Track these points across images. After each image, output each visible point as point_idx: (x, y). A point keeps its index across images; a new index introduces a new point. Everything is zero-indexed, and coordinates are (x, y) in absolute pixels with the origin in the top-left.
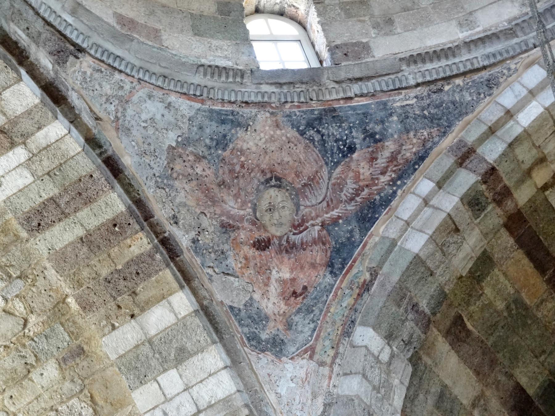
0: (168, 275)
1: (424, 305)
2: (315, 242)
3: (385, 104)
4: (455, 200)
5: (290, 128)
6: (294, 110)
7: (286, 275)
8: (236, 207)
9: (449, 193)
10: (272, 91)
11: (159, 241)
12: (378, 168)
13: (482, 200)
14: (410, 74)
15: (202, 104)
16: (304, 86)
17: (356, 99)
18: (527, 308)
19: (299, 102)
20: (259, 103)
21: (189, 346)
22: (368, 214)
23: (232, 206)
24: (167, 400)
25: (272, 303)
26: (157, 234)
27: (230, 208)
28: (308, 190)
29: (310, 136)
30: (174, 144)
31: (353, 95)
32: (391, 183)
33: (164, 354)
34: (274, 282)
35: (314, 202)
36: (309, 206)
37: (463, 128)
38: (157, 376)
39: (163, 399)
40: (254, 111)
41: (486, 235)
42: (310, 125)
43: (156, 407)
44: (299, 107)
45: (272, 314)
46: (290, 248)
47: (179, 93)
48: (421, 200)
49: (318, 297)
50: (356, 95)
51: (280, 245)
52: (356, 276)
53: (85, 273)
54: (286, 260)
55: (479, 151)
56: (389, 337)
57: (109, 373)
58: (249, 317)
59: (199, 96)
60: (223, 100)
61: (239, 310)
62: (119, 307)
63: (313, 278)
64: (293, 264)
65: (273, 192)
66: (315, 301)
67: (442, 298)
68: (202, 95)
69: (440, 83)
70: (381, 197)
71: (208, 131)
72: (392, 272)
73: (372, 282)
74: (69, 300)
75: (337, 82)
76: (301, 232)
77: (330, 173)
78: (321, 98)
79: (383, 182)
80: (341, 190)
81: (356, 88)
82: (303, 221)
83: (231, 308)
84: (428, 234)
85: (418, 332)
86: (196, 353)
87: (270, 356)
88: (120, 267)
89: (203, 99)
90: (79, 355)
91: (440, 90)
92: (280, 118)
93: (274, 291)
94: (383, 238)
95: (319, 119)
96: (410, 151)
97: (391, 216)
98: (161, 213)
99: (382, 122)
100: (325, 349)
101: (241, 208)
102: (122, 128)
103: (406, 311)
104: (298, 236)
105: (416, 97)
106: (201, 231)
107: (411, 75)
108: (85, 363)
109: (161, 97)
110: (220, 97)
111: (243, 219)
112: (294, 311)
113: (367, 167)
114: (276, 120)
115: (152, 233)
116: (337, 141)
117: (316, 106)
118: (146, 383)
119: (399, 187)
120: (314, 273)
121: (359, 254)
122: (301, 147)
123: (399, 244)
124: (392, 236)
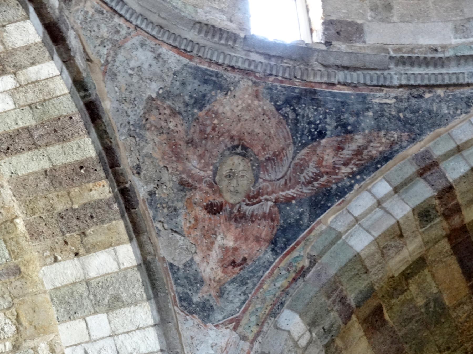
0: (120, 226)
1: (352, 299)
2: (264, 217)
3: (365, 97)
4: (408, 209)
5: (268, 101)
6: (276, 84)
7: (230, 243)
8: (198, 167)
9: (403, 200)
10: (260, 61)
11: (119, 190)
12: (342, 158)
13: (433, 212)
14: (396, 74)
15: (191, 60)
16: (292, 63)
17: (338, 86)
18: (443, 307)
19: (283, 77)
20: (245, 70)
21: (124, 296)
22: (321, 201)
23: (194, 165)
24: (91, 341)
25: (210, 268)
26: (119, 183)
27: (192, 167)
28: (270, 165)
29: (286, 113)
30: (154, 96)
31: (336, 82)
32: (351, 176)
33: (99, 297)
34: (217, 247)
35: (273, 178)
36: (267, 181)
37: (433, 140)
38: (87, 316)
39: (87, 339)
40: (238, 76)
41: (426, 243)
42: (288, 102)
43: (79, 344)
44: (281, 82)
45: (208, 279)
46: (239, 217)
47: (171, 45)
48: (375, 201)
49: (254, 271)
50: (339, 83)
51: (231, 212)
52: (295, 260)
53: (41, 203)
54: (233, 228)
55: (442, 165)
56: (312, 324)
57: (40, 298)
58: (186, 278)
59: (189, 52)
60: (211, 60)
61: (178, 269)
62: (66, 243)
63: (255, 252)
64: (239, 234)
65: (237, 160)
66: (251, 274)
67: (370, 293)
68: (192, 52)
69: (422, 89)
70: (338, 187)
71: (189, 88)
72: (332, 264)
73: (309, 269)
74: (17, 221)
75: (324, 66)
76: (254, 204)
77: (295, 153)
78: (305, 78)
79: (343, 173)
80: (302, 172)
81: (340, 76)
82: (259, 194)
83: (171, 265)
84: (374, 236)
85: (340, 321)
86: (130, 305)
87: (196, 320)
88: (76, 206)
89: (191, 56)
90: (14, 274)
91: (421, 97)
92: (261, 89)
93: (215, 256)
94: (330, 228)
95: (298, 98)
96: (376, 149)
97: (343, 208)
98: (127, 161)
99: (358, 115)
100: (249, 325)
101: (202, 169)
102: (110, 73)
103: (334, 302)
104: (250, 207)
105: (396, 98)
106: (160, 184)
107: (397, 75)
108: (18, 283)
109: (153, 46)
110: (209, 56)
111: (202, 180)
112: (229, 280)
113: (332, 154)
114: (257, 91)
115: (114, 181)
116: (310, 123)
117: (298, 84)
118: (74, 319)
119: (358, 181)
120: (256, 247)
121: (303, 238)
122: (274, 121)
123: (344, 237)
124: (340, 229)
